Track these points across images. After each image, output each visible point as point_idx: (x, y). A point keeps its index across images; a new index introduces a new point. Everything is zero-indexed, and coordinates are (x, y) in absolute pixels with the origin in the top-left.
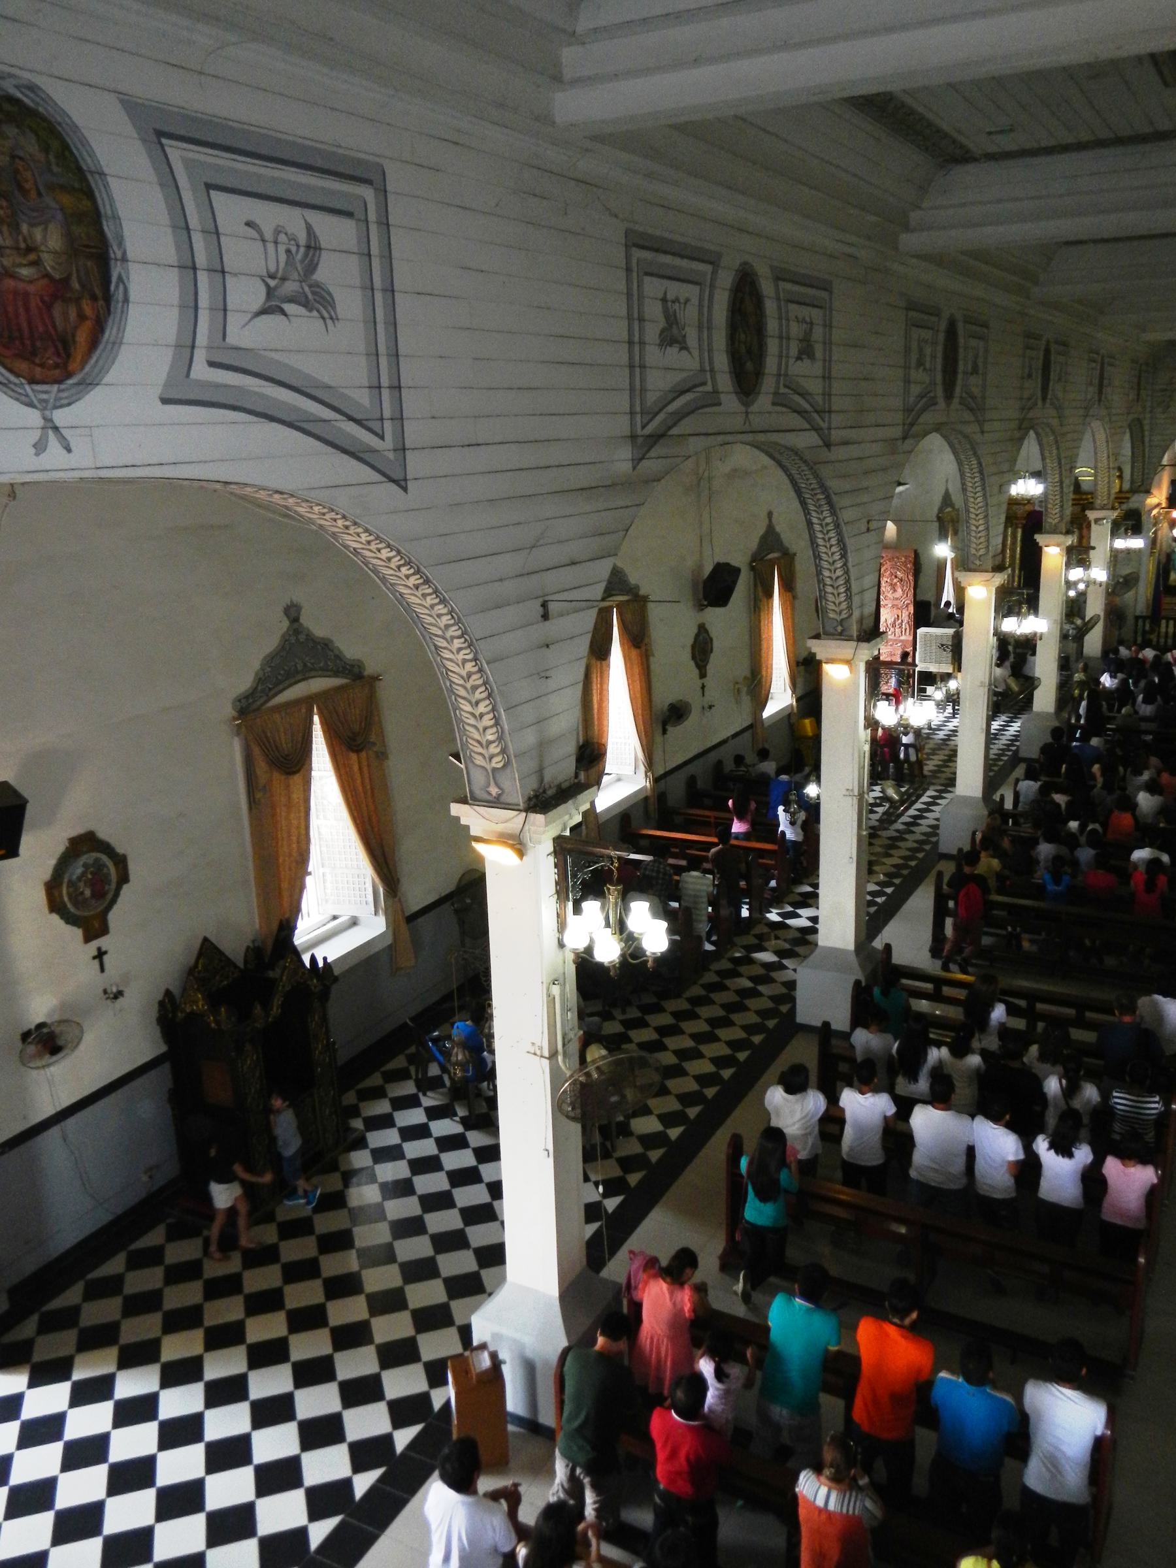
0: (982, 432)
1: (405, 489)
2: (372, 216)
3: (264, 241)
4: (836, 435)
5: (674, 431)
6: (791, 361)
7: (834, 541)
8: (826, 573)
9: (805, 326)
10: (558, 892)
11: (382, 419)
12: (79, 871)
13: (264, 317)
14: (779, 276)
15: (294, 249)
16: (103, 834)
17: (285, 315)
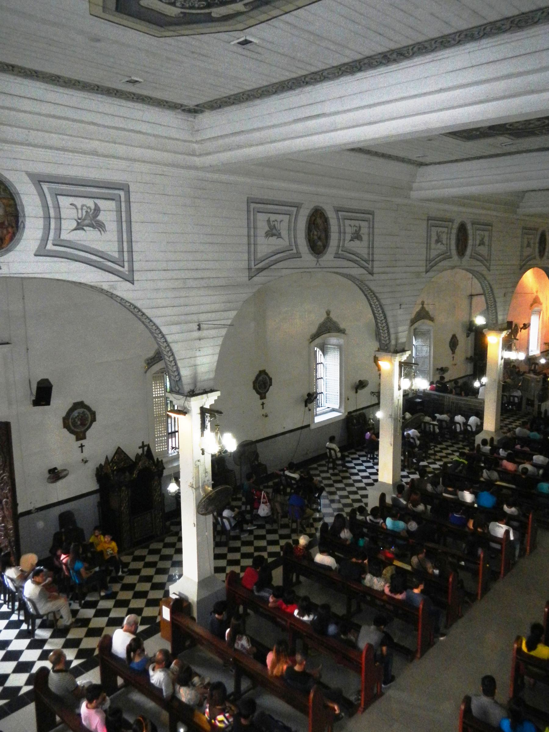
0: (489, 270)
1: (133, 284)
2: (123, 199)
3: (77, 209)
4: (375, 270)
5: (271, 267)
6: (346, 242)
7: (380, 312)
8: (380, 325)
9: (355, 228)
10: (201, 428)
11: (124, 261)
12: (76, 415)
13: (75, 232)
14: (338, 210)
15: (89, 211)
16: (87, 403)
17: (84, 230)
